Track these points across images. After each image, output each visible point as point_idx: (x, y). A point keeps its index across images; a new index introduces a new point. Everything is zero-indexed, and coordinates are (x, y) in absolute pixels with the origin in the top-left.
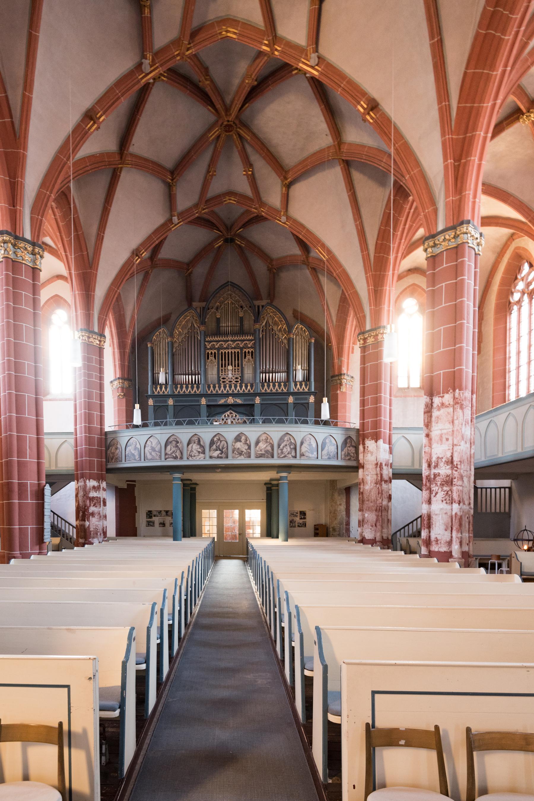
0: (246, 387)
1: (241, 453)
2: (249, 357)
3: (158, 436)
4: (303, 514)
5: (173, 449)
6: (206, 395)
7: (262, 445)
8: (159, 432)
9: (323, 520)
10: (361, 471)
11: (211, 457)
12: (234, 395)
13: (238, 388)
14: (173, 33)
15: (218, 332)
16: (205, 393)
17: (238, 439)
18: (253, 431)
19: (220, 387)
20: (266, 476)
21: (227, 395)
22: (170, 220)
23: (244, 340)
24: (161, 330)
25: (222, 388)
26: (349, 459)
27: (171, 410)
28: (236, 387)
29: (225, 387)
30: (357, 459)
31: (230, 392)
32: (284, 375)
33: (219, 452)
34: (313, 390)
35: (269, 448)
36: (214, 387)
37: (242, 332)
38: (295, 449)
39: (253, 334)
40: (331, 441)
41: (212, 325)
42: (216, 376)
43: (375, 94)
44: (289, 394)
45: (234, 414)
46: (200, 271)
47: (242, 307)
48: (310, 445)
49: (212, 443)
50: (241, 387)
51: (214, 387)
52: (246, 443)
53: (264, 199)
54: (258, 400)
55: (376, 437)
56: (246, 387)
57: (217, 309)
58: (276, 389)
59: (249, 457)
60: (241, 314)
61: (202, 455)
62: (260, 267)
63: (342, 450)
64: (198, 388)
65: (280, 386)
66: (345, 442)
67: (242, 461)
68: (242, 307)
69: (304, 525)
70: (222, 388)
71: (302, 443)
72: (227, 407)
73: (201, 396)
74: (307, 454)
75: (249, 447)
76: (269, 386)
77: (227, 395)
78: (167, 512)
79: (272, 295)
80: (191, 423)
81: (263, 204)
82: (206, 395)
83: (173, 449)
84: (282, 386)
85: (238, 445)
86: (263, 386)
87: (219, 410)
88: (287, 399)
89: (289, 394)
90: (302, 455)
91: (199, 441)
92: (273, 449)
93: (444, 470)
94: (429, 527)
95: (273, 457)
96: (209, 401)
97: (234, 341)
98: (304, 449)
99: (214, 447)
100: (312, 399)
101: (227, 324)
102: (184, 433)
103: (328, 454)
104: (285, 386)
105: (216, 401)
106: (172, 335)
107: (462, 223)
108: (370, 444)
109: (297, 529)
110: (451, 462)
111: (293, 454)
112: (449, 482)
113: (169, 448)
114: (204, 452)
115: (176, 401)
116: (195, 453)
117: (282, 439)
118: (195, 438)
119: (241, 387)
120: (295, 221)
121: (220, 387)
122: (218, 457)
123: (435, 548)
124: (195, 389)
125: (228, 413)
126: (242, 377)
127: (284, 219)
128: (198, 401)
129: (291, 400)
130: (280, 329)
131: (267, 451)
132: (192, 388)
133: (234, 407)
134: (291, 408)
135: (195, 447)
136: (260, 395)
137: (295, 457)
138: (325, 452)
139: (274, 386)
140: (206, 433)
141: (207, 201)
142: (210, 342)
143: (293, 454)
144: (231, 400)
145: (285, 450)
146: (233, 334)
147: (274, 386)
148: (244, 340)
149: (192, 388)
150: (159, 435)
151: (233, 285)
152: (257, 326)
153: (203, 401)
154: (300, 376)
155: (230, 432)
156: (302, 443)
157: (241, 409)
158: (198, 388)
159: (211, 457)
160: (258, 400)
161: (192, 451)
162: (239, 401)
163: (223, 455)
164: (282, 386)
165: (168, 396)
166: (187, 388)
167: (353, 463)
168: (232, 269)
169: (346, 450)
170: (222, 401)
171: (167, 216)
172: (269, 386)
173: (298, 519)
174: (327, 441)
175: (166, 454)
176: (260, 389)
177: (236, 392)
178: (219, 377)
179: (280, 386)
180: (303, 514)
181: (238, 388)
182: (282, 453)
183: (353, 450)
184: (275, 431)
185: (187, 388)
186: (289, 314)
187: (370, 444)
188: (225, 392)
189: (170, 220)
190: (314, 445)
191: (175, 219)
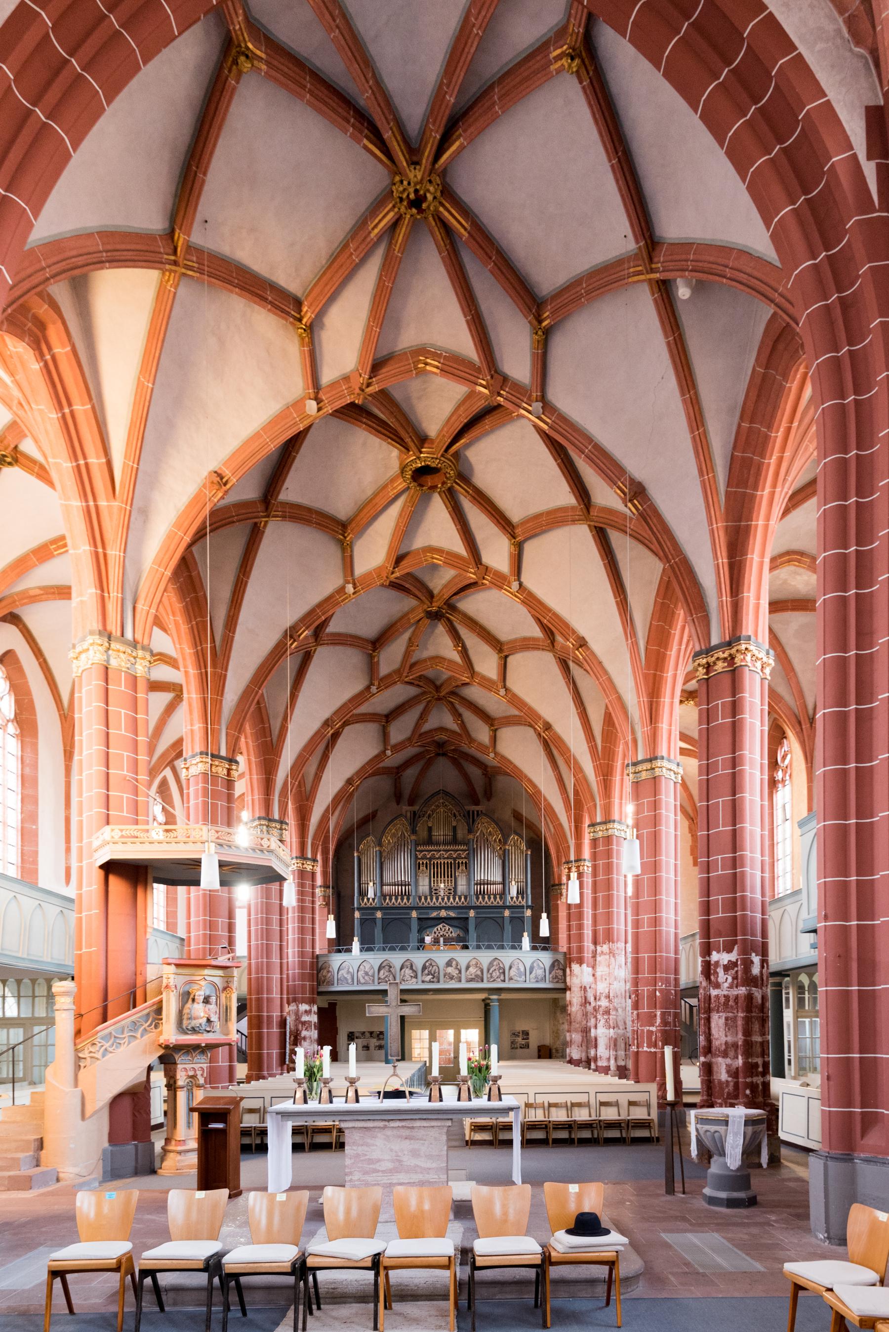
0: (460, 898)
1: (452, 978)
2: (463, 867)
3: (370, 961)
4: (526, 1034)
5: (387, 974)
6: (416, 908)
7: (472, 970)
8: (373, 956)
9: (548, 1041)
10: (568, 993)
11: (423, 982)
12: (447, 908)
13: (451, 899)
14: (396, 665)
15: (429, 841)
16: (416, 905)
17: (449, 964)
18: (463, 957)
19: (431, 899)
20: (483, 996)
21: (440, 908)
22: (384, 752)
23: (457, 851)
24: (369, 839)
25: (434, 899)
26: (557, 982)
27: (379, 924)
28: (449, 899)
29: (437, 899)
30: (565, 982)
31: (443, 904)
32: (500, 887)
33: (430, 977)
34: (530, 903)
35: (479, 973)
36: (426, 899)
37: (455, 841)
38: (504, 973)
39: (466, 844)
40: (538, 965)
41: (424, 834)
42: (427, 888)
43: (550, 719)
44: (505, 907)
45: (447, 927)
46: (410, 774)
47: (455, 815)
48: (518, 969)
49: (424, 968)
50: (454, 899)
51: (426, 899)
52: (457, 968)
53: (474, 734)
54: (472, 913)
55: (580, 961)
56: (460, 898)
57: (429, 816)
58: (491, 902)
59: (460, 981)
60: (454, 824)
61: (414, 980)
62: (474, 772)
63: (550, 973)
64: (408, 899)
65: (495, 898)
66: (553, 966)
67: (453, 985)
68: (455, 815)
69: (527, 1046)
70: (434, 899)
71: (510, 968)
72: (440, 920)
73: (412, 908)
74: (515, 978)
75: (460, 972)
76: (483, 898)
77: (440, 908)
78: (371, 1033)
79: (489, 793)
80: (403, 949)
81: (471, 740)
82: (416, 908)
83: (387, 974)
84: (498, 899)
85: (449, 970)
86: (478, 898)
87: (430, 923)
88: (502, 913)
89: (505, 907)
90: (511, 979)
91: (412, 966)
92: (482, 973)
93: (604, 1003)
94: (596, 1047)
95: (482, 981)
96: (420, 914)
97: (447, 851)
98: (513, 972)
99: (426, 972)
100: (528, 913)
101: (439, 834)
102: (397, 958)
103: (536, 977)
104: (501, 898)
105: (428, 913)
106: (380, 844)
107: (610, 822)
108: (575, 967)
109: (519, 1051)
110: (608, 997)
111: (502, 978)
112: (607, 1012)
113: (382, 972)
114: (416, 977)
115: (384, 914)
116: (407, 977)
117: (491, 964)
118: (408, 963)
119: (454, 899)
120: (503, 757)
121: (431, 899)
122: (430, 982)
123: (600, 1064)
124: (405, 900)
125: (441, 926)
126: (455, 888)
127: (492, 755)
128: (408, 914)
129: (507, 913)
130: (495, 840)
131: (477, 976)
132: (402, 899)
133: (446, 920)
134: (507, 922)
135: (408, 972)
136: (474, 908)
137: (504, 981)
138: (533, 975)
139: (489, 898)
140: (419, 959)
141: (421, 735)
142: (422, 851)
143: (502, 978)
144: (443, 914)
145: (494, 974)
146: (445, 843)
147: (489, 898)
148: (457, 851)
149: (402, 899)
150: (375, 959)
151: (446, 793)
152: (471, 837)
153: (414, 914)
154: (514, 891)
155: (441, 957)
156: (510, 968)
157: (455, 923)
158: (408, 899)
159: (423, 982)
160: (472, 913)
161: (404, 976)
162: (452, 914)
163: (435, 980)
164: (498, 899)
165: (376, 909)
166: (396, 899)
167: (561, 986)
168: (444, 774)
169: (553, 973)
170: (434, 914)
171: (381, 748)
172: (483, 898)
173: (519, 1040)
174: (535, 965)
175: (379, 979)
176: (474, 901)
177: (449, 904)
178: (431, 888)
179: (495, 898)
180: (526, 1034)
181: (451, 899)
182: (491, 977)
183: (560, 973)
184: (485, 957)
185: (396, 899)
186: (507, 816)
187: (575, 967)
188: (437, 904)
189: (384, 752)
190: (522, 969)
191: (389, 753)
